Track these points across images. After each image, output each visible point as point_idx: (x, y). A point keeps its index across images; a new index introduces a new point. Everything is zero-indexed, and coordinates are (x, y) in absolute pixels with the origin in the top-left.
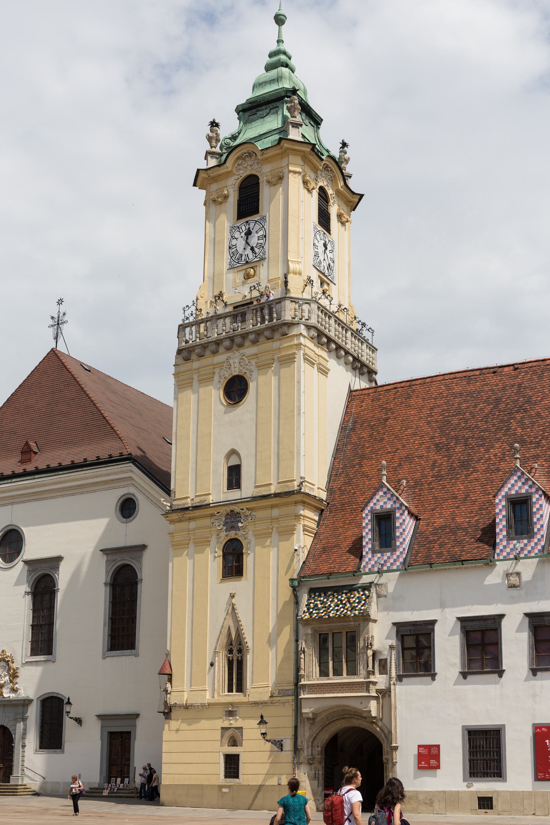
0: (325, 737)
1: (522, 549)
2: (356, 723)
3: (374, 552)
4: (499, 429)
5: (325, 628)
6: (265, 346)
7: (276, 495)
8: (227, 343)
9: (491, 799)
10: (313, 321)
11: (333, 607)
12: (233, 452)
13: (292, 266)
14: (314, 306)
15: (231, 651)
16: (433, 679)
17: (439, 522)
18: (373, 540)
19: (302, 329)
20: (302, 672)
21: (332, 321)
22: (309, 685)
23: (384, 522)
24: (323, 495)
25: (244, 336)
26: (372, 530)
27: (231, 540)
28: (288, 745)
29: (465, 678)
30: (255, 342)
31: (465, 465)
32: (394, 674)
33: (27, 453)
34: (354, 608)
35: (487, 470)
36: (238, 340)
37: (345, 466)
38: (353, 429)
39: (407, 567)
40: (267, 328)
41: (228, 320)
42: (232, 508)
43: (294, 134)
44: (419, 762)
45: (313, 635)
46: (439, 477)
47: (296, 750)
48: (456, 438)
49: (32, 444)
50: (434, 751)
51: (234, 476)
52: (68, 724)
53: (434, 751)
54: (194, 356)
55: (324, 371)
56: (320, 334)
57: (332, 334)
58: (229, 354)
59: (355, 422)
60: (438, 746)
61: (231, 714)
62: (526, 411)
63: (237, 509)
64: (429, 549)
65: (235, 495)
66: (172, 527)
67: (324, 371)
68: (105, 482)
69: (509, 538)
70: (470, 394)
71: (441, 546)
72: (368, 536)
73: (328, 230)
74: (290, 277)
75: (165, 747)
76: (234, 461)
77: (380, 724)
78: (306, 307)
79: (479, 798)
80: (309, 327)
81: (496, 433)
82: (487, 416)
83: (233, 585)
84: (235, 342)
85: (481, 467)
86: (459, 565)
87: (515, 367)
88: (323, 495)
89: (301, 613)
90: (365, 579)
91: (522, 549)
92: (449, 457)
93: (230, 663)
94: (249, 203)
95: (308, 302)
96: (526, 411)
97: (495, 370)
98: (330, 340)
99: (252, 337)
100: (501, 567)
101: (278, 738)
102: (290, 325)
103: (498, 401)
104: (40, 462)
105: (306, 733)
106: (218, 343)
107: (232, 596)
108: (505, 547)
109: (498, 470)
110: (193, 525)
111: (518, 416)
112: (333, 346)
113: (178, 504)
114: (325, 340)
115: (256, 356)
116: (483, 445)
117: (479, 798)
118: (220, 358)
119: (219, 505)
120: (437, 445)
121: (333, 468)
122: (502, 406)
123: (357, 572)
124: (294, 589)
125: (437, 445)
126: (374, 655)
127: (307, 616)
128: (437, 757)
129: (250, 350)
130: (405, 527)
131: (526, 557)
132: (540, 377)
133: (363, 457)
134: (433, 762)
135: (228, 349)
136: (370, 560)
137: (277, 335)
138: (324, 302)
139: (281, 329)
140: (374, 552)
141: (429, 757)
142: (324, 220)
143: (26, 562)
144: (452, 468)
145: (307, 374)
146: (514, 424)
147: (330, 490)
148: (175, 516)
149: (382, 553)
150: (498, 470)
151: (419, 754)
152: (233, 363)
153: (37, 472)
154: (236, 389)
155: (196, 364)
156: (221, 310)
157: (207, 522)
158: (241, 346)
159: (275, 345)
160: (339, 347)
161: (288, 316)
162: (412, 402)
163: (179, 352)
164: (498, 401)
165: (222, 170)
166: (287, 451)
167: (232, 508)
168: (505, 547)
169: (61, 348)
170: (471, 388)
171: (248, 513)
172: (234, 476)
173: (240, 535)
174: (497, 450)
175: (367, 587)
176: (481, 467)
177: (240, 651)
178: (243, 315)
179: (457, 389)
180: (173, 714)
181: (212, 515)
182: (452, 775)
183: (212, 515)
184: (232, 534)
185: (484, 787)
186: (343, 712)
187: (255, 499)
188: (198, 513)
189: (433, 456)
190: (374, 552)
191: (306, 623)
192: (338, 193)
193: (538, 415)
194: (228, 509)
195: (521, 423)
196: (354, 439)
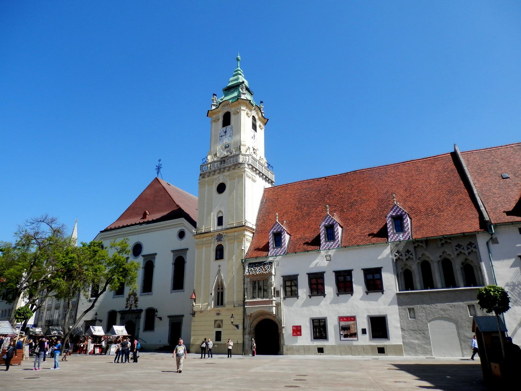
0: (255, 323)
1: (331, 246)
2: (268, 317)
3: (274, 248)
4: (320, 201)
5: (255, 279)
6: (232, 171)
7: (236, 227)
8: (218, 171)
9: (322, 348)
10: (250, 162)
11: (258, 271)
12: (220, 211)
13: (242, 143)
14: (250, 157)
15: (219, 289)
16: (298, 298)
17: (298, 236)
19: (246, 166)
20: (246, 297)
21: (257, 163)
22: (249, 302)
24: (254, 227)
25: (224, 168)
26: (273, 240)
27: (219, 245)
28: (241, 327)
29: (310, 298)
30: (229, 170)
31: (308, 214)
32: (282, 297)
33: (145, 216)
34: (266, 270)
35: (317, 216)
36: (222, 170)
37: (262, 216)
38: (266, 202)
39: (286, 254)
40: (233, 165)
41: (219, 163)
42: (220, 232)
43: (243, 97)
44: (293, 333)
45: (250, 281)
46: (298, 219)
47: (244, 328)
48: (304, 204)
49: (147, 212)
50: (299, 329)
51: (220, 221)
52: (157, 320)
53: (299, 329)
54: (206, 176)
55: (254, 181)
56: (253, 167)
57: (257, 168)
58: (219, 175)
59: (266, 200)
60: (300, 326)
61: (218, 314)
62: (330, 194)
63: (221, 233)
64: (295, 247)
65: (220, 228)
66: (197, 240)
67: (254, 181)
68: (174, 225)
69: (326, 242)
70: (309, 188)
71: (299, 245)
72: (271, 242)
73: (256, 131)
74: (242, 147)
75: (192, 328)
76: (220, 215)
77: (277, 317)
78: (247, 157)
79: (318, 348)
80: (248, 165)
81: (319, 202)
83: (220, 262)
84: (221, 171)
85: (314, 215)
86: (306, 253)
87: (325, 178)
88: (254, 227)
89: (246, 273)
90: (271, 259)
91: (331, 246)
93: (218, 293)
94: (227, 120)
95: (248, 155)
96: (330, 194)
97: (318, 179)
98: (256, 170)
99: (227, 169)
100: (323, 253)
101: (237, 324)
102: (241, 164)
103: (320, 190)
104: (149, 218)
105: (248, 322)
106: (215, 171)
107: (219, 266)
108: (324, 245)
109: (321, 216)
110: (204, 239)
111: (328, 196)
112: (258, 172)
113: (199, 232)
114: (254, 169)
115: (229, 176)
116: (314, 207)
117: (318, 348)
118: (216, 176)
119: (214, 231)
121: (258, 217)
123: (267, 256)
124: (243, 263)
126: (274, 289)
127: (248, 274)
128: (300, 331)
129: (226, 173)
130: (286, 238)
131: (333, 249)
132: (335, 181)
133: (269, 213)
134: (298, 333)
135: (219, 173)
136: (272, 251)
137: (237, 167)
138: (254, 156)
139: (238, 165)
140: (274, 248)
141: (297, 331)
142: (254, 127)
143: (143, 256)
144: (303, 216)
145: (248, 182)
147: (257, 225)
148: (198, 236)
149: (277, 248)
150: (321, 216)
151: (293, 330)
152: (220, 179)
153: (148, 222)
154: (221, 188)
155: (207, 179)
156: (215, 159)
157: (210, 238)
158: (223, 172)
159: (236, 171)
160: (260, 172)
161: (241, 161)
163: (201, 175)
164: (320, 190)
165: (217, 110)
166: (240, 210)
167: (220, 232)
168: (324, 245)
169: (159, 178)
170: (310, 186)
171: (226, 234)
172: (220, 221)
173: (222, 243)
174: (320, 209)
175: (271, 263)
176: (314, 215)
177: (222, 289)
178: (224, 161)
179: (304, 187)
180: (196, 315)
181: (212, 236)
182: (306, 338)
183: (212, 236)
184: (219, 243)
185: (320, 343)
186: (262, 313)
187: (228, 229)
188: (206, 235)
189: (296, 211)
191: (248, 276)
192: (259, 118)
193: (335, 195)
194: (218, 233)
195: (329, 198)
196: (266, 206)
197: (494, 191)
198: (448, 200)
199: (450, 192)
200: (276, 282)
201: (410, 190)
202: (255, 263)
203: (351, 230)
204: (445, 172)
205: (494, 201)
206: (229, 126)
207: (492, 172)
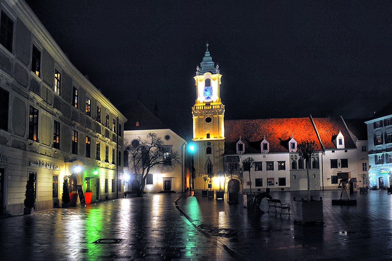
15: (208, 166)
18: (238, 149)
23: (241, 146)
48: (247, 132)
82: (252, 128)
83: (209, 155)
92: (247, 135)
109: (257, 138)
120: (244, 133)
122: (254, 127)
125: (244, 133)
146: (258, 131)
162: (237, 124)
167: (209, 141)
170: (247, 123)
176: (253, 137)
190: (239, 151)
195: (259, 130)
197: (324, 136)
198: (309, 138)
199: (309, 134)
200: (241, 164)
201: (294, 131)
202: (229, 157)
203: (272, 146)
204: (307, 126)
205: (324, 140)
206: (210, 87)
207: (323, 128)
